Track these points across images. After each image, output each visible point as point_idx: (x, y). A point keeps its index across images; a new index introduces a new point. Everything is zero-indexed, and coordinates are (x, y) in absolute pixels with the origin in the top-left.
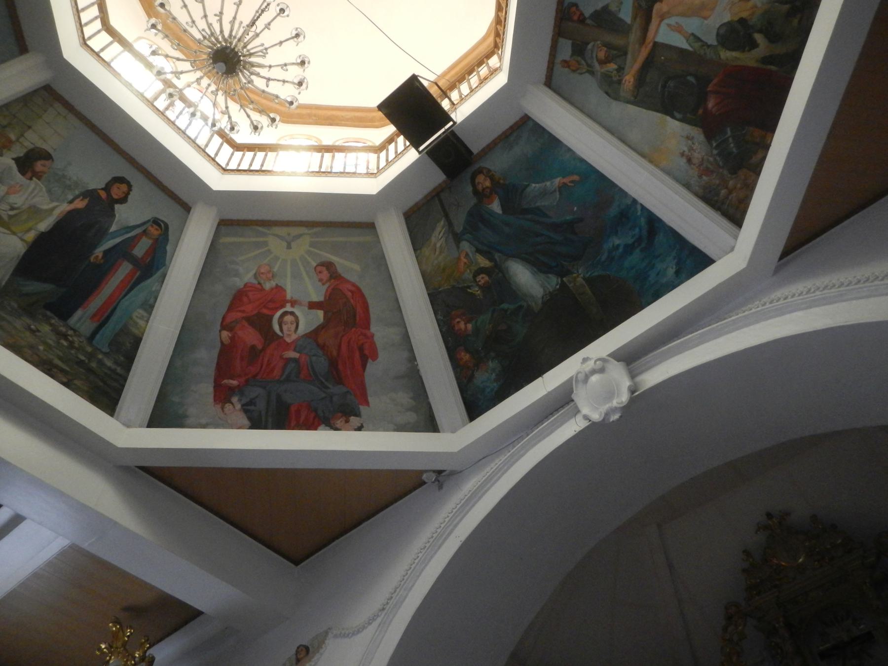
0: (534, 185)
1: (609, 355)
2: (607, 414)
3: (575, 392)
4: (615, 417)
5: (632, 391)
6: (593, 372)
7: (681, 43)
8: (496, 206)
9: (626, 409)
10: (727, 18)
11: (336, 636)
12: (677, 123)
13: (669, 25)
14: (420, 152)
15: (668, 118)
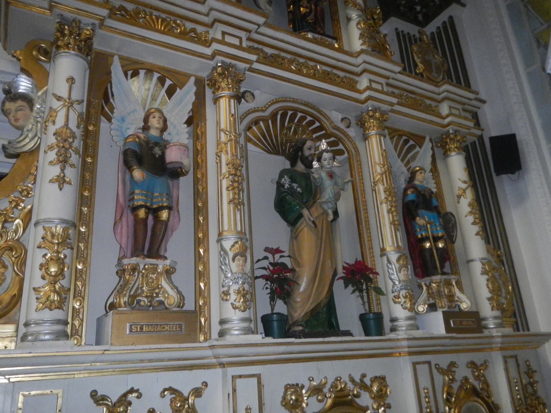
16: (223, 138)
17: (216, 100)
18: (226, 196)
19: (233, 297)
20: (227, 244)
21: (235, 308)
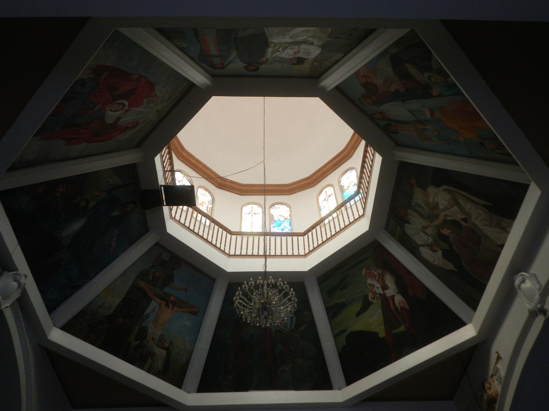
0: (117, 232)
7: (147, 312)
8: (116, 213)
10: (149, 331)
12: (118, 304)
13: (156, 307)
14: (161, 186)
15: (121, 300)
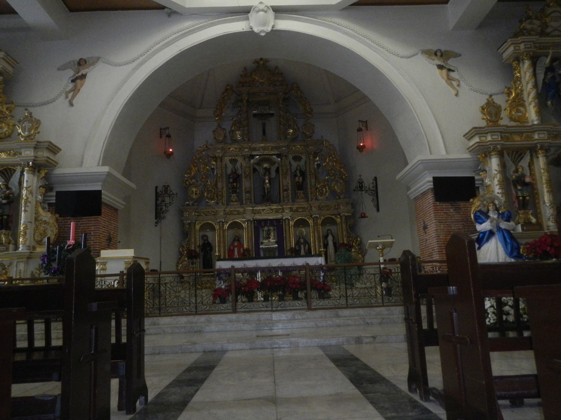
1: (270, 6)
2: (261, 32)
3: (251, 13)
4: (263, 34)
5: (273, 27)
6: (262, 10)
9: (268, 34)
11: (103, 62)
16: (542, 171)
17: (538, 157)
18: (545, 190)
19: (551, 219)
20: (548, 205)
21: (552, 222)
